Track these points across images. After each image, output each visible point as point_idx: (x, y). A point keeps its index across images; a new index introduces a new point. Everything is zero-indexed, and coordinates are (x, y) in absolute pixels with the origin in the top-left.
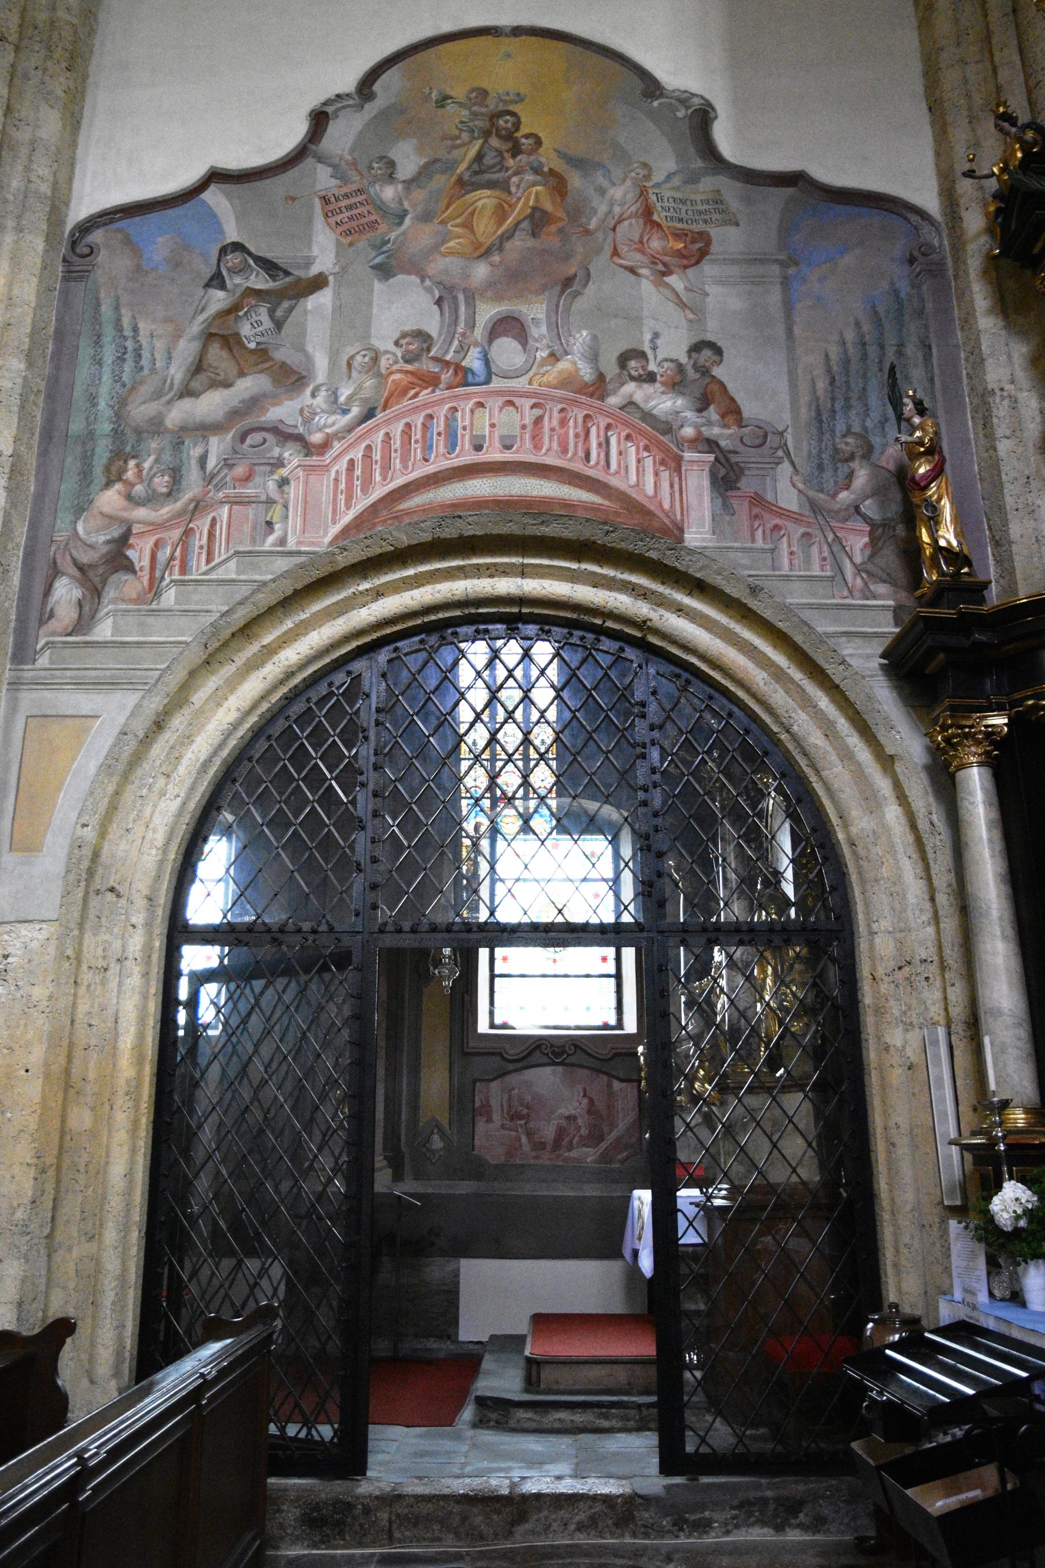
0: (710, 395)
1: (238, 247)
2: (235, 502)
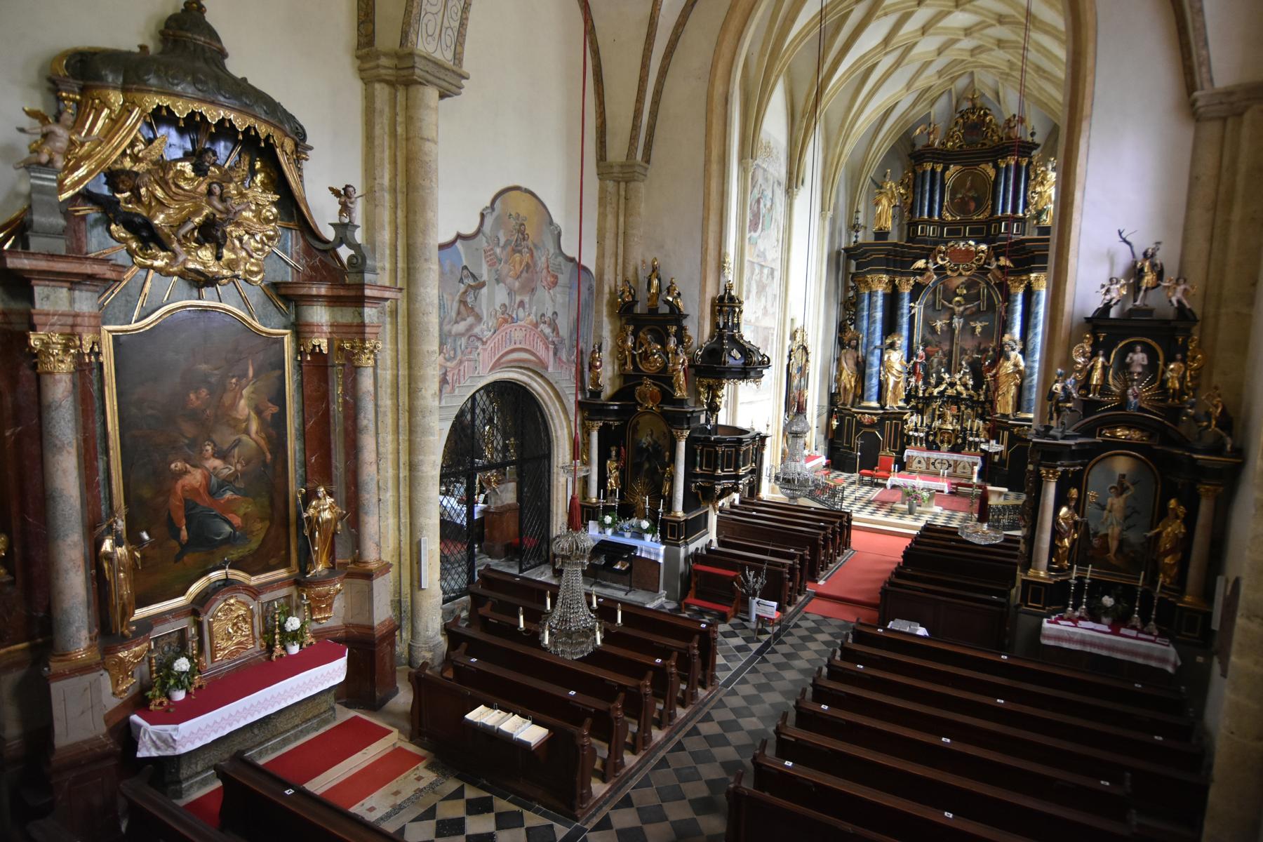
0: (555, 329)
1: (465, 268)
2: (469, 360)
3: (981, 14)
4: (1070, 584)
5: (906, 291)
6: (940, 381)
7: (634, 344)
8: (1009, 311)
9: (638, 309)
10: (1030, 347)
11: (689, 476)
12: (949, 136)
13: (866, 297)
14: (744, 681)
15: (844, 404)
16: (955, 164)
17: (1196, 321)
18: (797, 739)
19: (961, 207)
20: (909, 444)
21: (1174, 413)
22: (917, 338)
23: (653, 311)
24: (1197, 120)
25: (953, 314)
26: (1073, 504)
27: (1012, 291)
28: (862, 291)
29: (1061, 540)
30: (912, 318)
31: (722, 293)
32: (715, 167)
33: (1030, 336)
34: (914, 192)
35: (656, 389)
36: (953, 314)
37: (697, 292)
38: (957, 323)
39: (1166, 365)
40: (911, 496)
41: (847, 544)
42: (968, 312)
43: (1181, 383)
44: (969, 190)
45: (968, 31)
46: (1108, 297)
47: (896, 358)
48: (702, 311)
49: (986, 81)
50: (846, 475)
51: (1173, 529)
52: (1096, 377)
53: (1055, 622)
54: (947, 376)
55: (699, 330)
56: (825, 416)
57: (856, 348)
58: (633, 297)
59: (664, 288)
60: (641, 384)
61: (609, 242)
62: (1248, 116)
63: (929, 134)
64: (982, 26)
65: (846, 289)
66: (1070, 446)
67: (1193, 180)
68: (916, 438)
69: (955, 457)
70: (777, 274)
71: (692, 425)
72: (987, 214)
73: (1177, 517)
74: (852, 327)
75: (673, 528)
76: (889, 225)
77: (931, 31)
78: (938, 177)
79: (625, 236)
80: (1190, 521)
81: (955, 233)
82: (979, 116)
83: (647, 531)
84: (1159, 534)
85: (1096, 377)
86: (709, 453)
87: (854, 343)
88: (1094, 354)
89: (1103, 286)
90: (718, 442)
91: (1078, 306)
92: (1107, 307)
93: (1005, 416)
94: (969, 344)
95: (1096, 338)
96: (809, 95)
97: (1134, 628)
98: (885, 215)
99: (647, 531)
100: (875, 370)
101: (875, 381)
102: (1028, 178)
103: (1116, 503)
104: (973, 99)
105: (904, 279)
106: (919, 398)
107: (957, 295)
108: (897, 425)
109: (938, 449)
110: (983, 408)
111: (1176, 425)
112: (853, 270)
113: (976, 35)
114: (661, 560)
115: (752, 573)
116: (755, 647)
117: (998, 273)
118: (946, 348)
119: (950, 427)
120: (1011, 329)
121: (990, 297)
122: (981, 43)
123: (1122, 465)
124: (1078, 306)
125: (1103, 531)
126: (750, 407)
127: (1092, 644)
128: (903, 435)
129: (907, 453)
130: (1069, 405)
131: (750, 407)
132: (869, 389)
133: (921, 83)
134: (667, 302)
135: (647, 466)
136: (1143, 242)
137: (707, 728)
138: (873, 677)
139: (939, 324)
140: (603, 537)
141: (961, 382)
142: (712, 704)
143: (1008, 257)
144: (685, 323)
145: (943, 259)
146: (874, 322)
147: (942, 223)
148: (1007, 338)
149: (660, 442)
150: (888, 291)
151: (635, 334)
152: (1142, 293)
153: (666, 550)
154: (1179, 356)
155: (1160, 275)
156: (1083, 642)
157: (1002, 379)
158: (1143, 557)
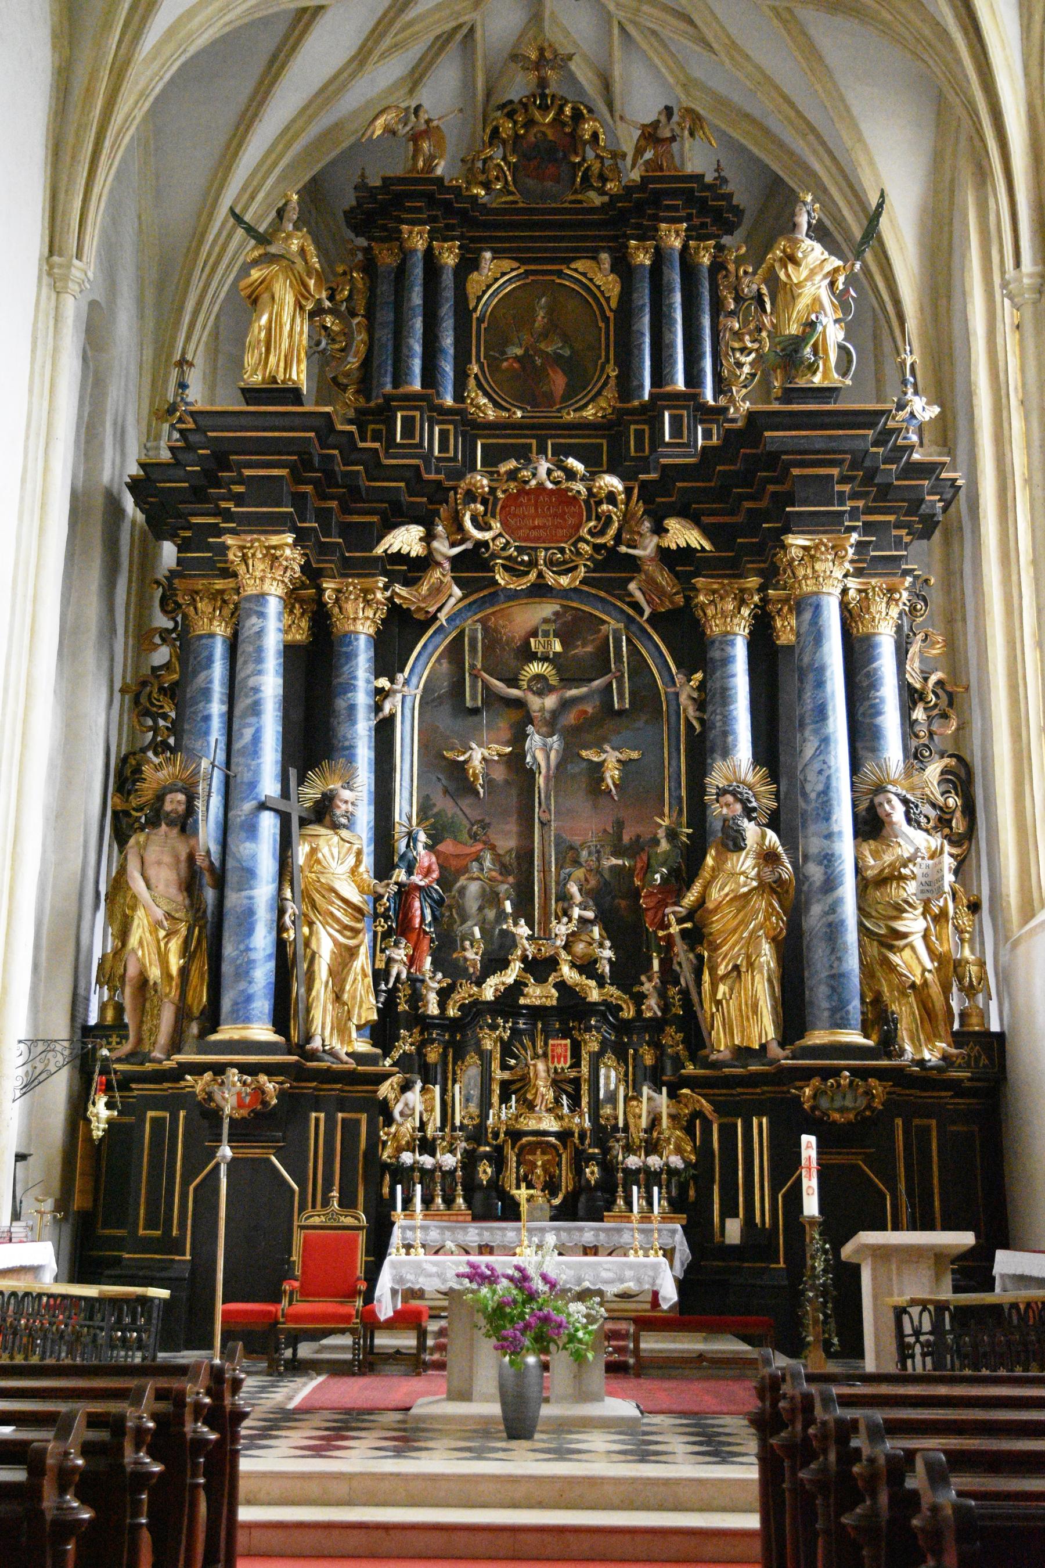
5: (361, 625)
6: (495, 963)
8: (712, 698)
12: (474, 168)
13: (219, 650)
16: (498, 254)
19: (524, 383)
27: (715, 628)
28: (201, 627)
30: (384, 730)
34: (370, 330)
38: (541, 750)
42: (570, 718)
44: (545, 335)
47: (340, 859)
54: (523, 930)
56: (59, 1086)
57: (185, 823)
65: (143, 638)
68: (427, 1175)
76: (300, 375)
78: (448, 279)
87: (175, 802)
93: (743, 1053)
94: (587, 826)
98: (284, 343)
100: (264, 890)
101: (262, 940)
102: (717, 307)
105: (354, 585)
107: (532, 657)
108: (350, 1129)
110: (657, 1045)
117: (664, 578)
118: (507, 842)
119: (549, 1124)
120: (726, 752)
121: (639, 667)
132: (244, 972)
139: (477, 756)
141: (572, 934)
143: (694, 519)
146: (255, 709)
147: (470, 427)
148: (717, 778)
150: (299, 636)
157: (718, 924)
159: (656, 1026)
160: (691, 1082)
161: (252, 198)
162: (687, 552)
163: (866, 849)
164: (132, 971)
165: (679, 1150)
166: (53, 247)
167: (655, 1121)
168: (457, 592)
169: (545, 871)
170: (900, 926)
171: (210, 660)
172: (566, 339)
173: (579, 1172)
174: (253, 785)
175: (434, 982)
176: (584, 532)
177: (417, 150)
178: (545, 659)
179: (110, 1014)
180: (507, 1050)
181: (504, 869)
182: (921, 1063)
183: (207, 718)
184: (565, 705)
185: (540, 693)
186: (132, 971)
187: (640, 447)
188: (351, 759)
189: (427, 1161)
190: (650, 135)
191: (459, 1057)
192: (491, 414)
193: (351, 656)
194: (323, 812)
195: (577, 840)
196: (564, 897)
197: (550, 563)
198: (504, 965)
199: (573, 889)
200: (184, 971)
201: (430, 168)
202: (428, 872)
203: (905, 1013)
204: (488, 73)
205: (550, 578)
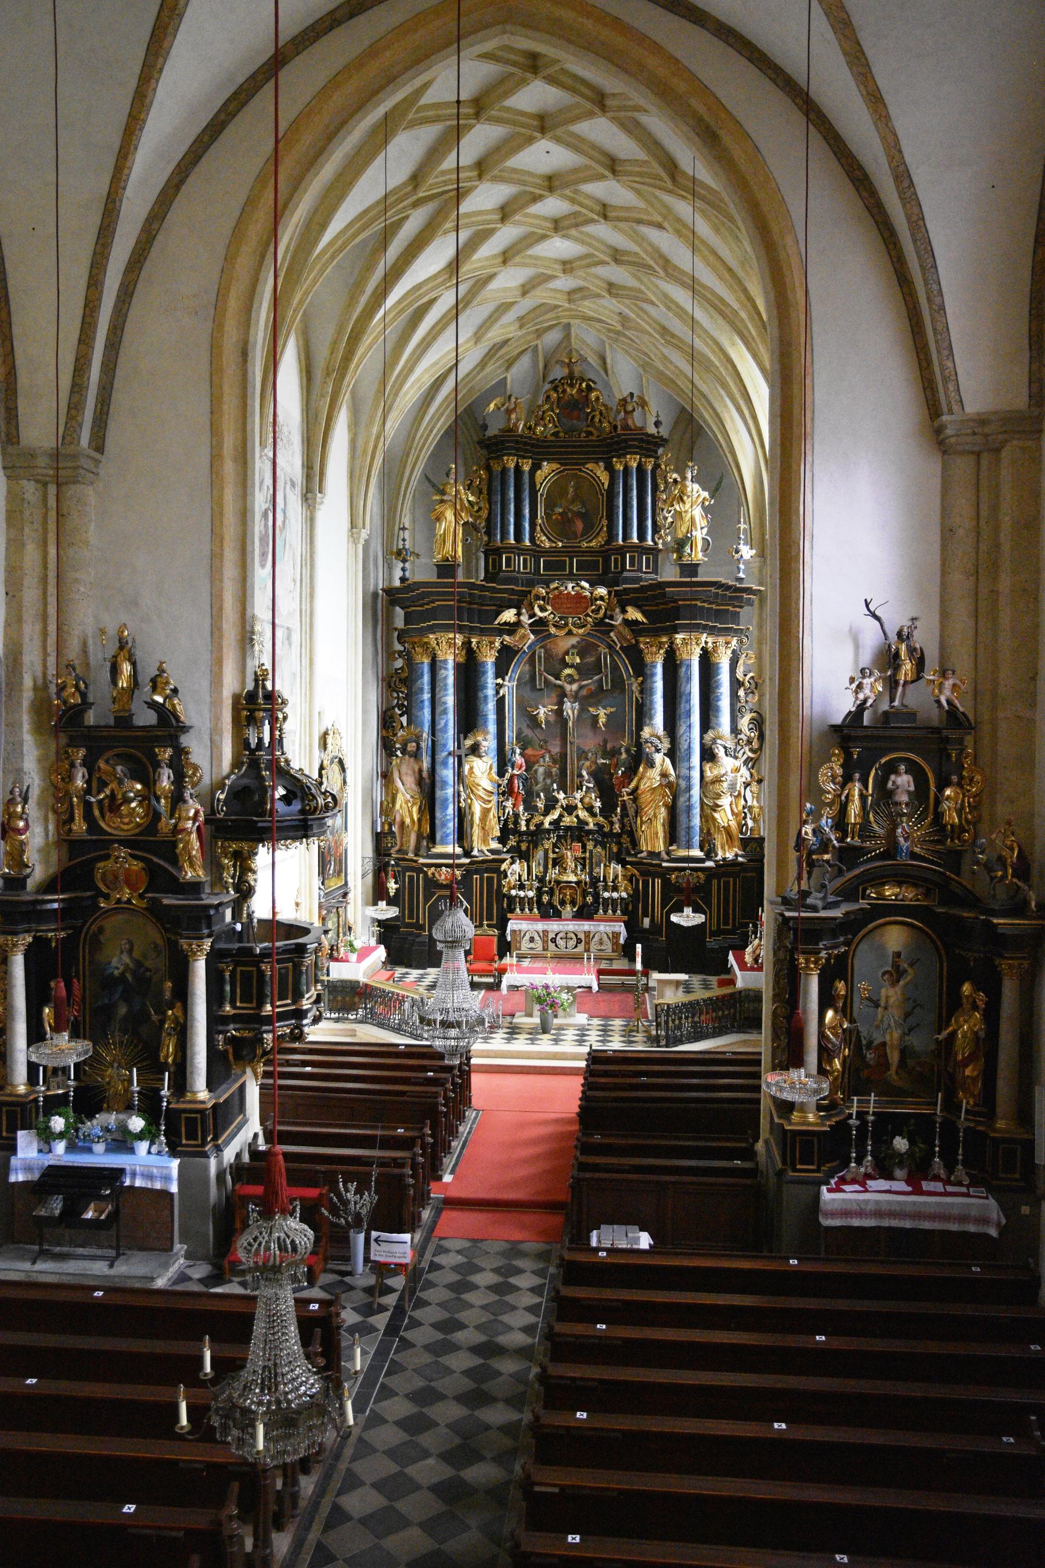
3: (590, 245)
4: (849, 1128)
5: (489, 659)
6: (551, 804)
7: (88, 782)
8: (646, 690)
9: (91, 718)
10: (684, 746)
11: (215, 1021)
13: (426, 669)
14: (386, 1393)
15: (399, 851)
16: (549, 460)
17: (971, 727)
18: (562, 1488)
19: (562, 527)
20: (512, 911)
21: (954, 859)
22: (510, 734)
23: (124, 721)
24: (945, 452)
25: (562, 695)
26: (840, 1004)
27: (648, 659)
28: (418, 658)
29: (830, 1062)
30: (500, 703)
31: (250, 686)
32: (229, 467)
33: (682, 729)
35: (136, 866)
36: (562, 695)
37: (205, 684)
38: (570, 709)
39: (941, 789)
40: (546, 1002)
41: (467, 1101)
42: (584, 692)
43: (960, 817)
44: (573, 502)
45: (567, 266)
46: (861, 696)
47: (482, 770)
48: (217, 718)
49: (586, 339)
50: (415, 973)
51: (967, 1026)
52: (854, 809)
53: (838, 1190)
54: (561, 796)
55: (212, 753)
57: (416, 755)
58: (84, 695)
59: (145, 678)
60: (107, 857)
61: (30, 595)
62: (1005, 454)
63: (509, 412)
64: (588, 261)
65: (390, 655)
66: (835, 919)
67: (947, 533)
68: (522, 899)
69: (586, 926)
70: (296, 637)
71: (216, 928)
72: (601, 539)
73: (975, 1007)
74: (404, 720)
75: (191, 1123)
77: (517, 259)
78: (526, 479)
79: (59, 582)
80: (992, 1015)
81: (556, 567)
82: (580, 390)
83: (140, 1136)
84: (953, 1034)
85: (854, 809)
86: (246, 977)
87: (411, 747)
88: (847, 779)
89: (852, 680)
90: (265, 954)
91: (817, 709)
92: (861, 708)
93: (652, 854)
94: (590, 742)
95: (848, 755)
96: (335, 342)
97: (936, 1178)
99: (140, 1136)
103: (892, 994)
104: (570, 365)
105: (486, 640)
106: (521, 834)
108: (490, 880)
109: (558, 915)
110: (619, 844)
111: (958, 874)
112: (399, 622)
113: (581, 273)
114: (174, 1188)
115: (353, 1187)
116: (380, 1321)
117: (626, 632)
118: (556, 750)
119: (572, 878)
120: (651, 718)
121: (615, 668)
122: (585, 284)
123: (895, 938)
124: (817, 709)
125: (878, 1040)
126: (284, 883)
127: (891, 1214)
128: (501, 896)
129: (512, 925)
130: (826, 857)
131: (284, 883)
132: (444, 825)
133: (495, 334)
134: (153, 705)
135: (123, 1010)
136: (895, 619)
137: (360, 1502)
138: (626, 1341)
139: (542, 712)
140: (49, 1160)
142: (348, 1452)
143: (638, 607)
144: (185, 740)
145: (543, 609)
146: (445, 712)
147: (536, 552)
148: (646, 733)
149: (148, 964)
150: (461, 660)
151: (89, 764)
152: (900, 689)
153: (180, 1166)
154: (955, 778)
155: (920, 664)
156: (878, 1214)
157: (645, 798)
158: (933, 1071)
159: (619, 836)
160: (631, 863)
161: (431, 431)
162: (636, 622)
163: (707, 767)
164: (398, 819)
165: (626, 890)
166: (353, 525)
167: (616, 877)
168: (532, 637)
169: (572, 764)
170: (719, 802)
171: (422, 675)
172: (584, 504)
173: (584, 898)
174: (445, 745)
175: (523, 818)
176: (589, 611)
177: (509, 419)
178: (572, 666)
179: (386, 827)
180: (555, 845)
181: (554, 761)
182: (724, 859)
183: (422, 702)
184: (581, 688)
185: (570, 683)
186: (398, 819)
187: (616, 567)
188: (486, 722)
189: (522, 894)
190: (624, 402)
191: (536, 847)
192: (548, 545)
193: (485, 673)
194: (475, 750)
195: (586, 749)
196: (580, 776)
197: (574, 624)
198: (554, 808)
199: (584, 773)
200: (419, 820)
201: (516, 425)
202: (520, 767)
203: (719, 840)
204: (545, 358)
205: (575, 630)
